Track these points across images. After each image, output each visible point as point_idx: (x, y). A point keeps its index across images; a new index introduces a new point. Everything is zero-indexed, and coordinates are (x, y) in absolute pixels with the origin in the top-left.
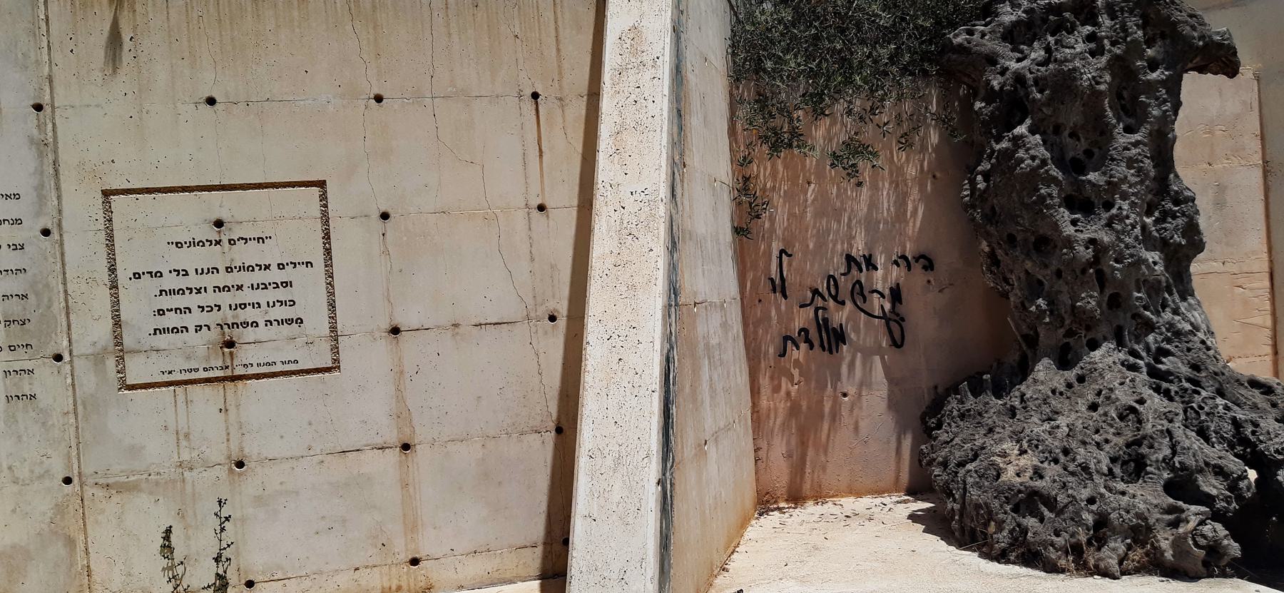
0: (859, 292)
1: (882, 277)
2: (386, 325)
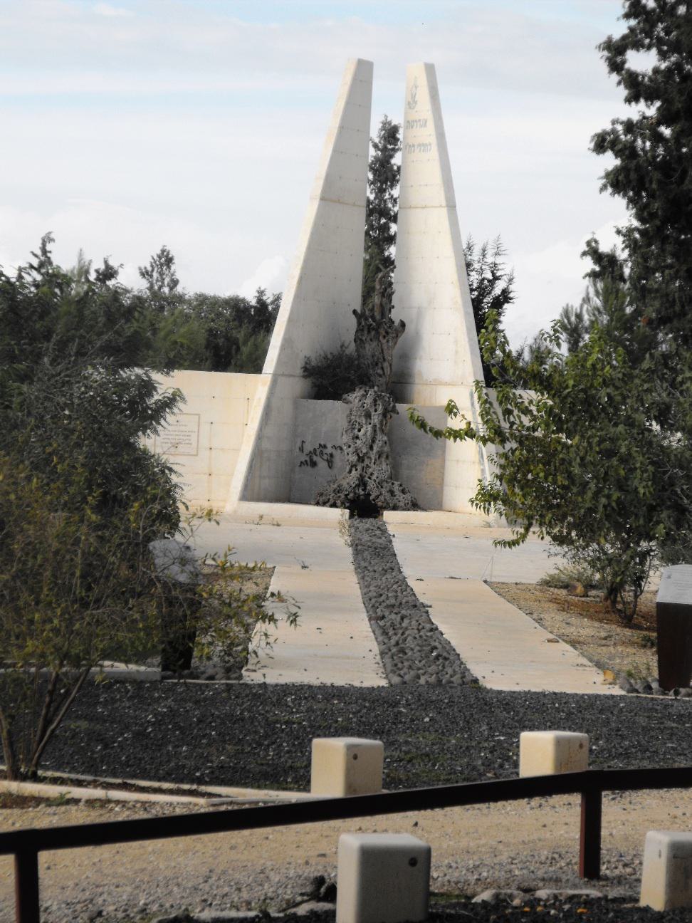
0: (322, 453)
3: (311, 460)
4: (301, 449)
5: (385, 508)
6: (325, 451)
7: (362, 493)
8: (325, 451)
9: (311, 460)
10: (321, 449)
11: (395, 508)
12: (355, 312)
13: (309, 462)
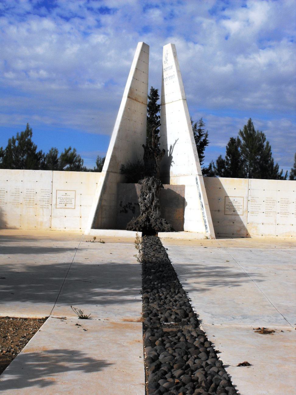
0: (130, 206)
2: (80, 205)
3: (125, 210)
4: (121, 205)
7: (148, 224)
9: (125, 210)
11: (163, 231)
12: (143, 146)
13: (124, 211)
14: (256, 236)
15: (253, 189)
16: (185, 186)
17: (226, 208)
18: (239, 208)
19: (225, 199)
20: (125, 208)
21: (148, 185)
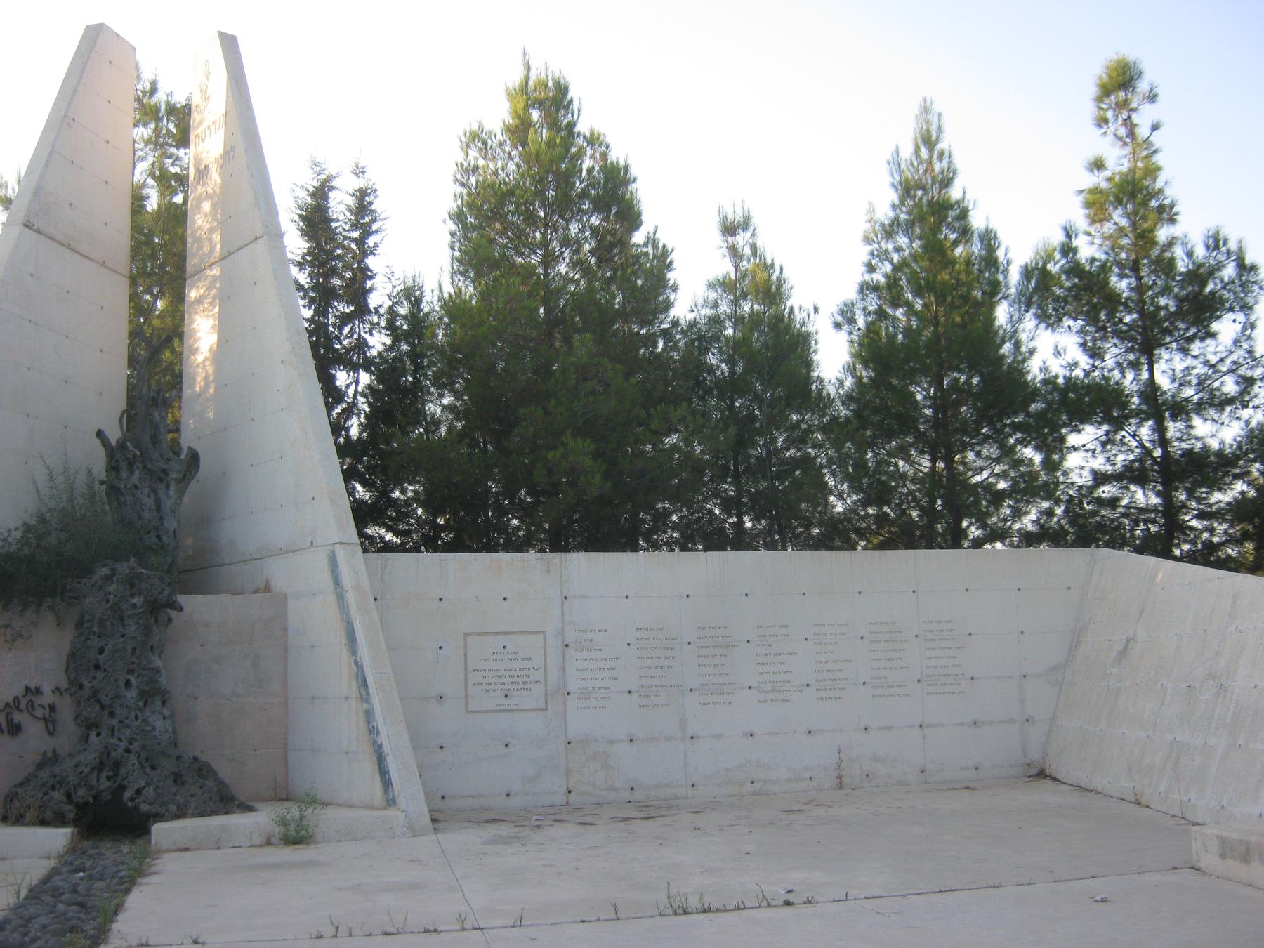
0: (31, 704)
1: (48, 698)
3: (10, 721)
5: (159, 817)
6: (39, 701)
7: (105, 784)
8: (39, 701)
9: (10, 721)
10: (29, 697)
14: (604, 793)
15: (582, 597)
16: (286, 597)
17: (470, 685)
18: (527, 679)
19: (465, 647)
20: (7, 715)
21: (108, 601)
